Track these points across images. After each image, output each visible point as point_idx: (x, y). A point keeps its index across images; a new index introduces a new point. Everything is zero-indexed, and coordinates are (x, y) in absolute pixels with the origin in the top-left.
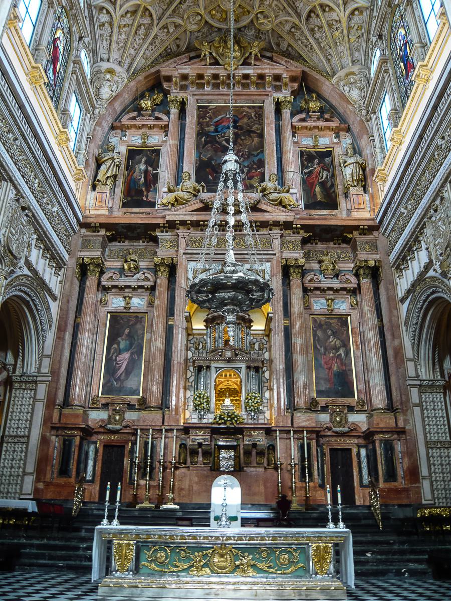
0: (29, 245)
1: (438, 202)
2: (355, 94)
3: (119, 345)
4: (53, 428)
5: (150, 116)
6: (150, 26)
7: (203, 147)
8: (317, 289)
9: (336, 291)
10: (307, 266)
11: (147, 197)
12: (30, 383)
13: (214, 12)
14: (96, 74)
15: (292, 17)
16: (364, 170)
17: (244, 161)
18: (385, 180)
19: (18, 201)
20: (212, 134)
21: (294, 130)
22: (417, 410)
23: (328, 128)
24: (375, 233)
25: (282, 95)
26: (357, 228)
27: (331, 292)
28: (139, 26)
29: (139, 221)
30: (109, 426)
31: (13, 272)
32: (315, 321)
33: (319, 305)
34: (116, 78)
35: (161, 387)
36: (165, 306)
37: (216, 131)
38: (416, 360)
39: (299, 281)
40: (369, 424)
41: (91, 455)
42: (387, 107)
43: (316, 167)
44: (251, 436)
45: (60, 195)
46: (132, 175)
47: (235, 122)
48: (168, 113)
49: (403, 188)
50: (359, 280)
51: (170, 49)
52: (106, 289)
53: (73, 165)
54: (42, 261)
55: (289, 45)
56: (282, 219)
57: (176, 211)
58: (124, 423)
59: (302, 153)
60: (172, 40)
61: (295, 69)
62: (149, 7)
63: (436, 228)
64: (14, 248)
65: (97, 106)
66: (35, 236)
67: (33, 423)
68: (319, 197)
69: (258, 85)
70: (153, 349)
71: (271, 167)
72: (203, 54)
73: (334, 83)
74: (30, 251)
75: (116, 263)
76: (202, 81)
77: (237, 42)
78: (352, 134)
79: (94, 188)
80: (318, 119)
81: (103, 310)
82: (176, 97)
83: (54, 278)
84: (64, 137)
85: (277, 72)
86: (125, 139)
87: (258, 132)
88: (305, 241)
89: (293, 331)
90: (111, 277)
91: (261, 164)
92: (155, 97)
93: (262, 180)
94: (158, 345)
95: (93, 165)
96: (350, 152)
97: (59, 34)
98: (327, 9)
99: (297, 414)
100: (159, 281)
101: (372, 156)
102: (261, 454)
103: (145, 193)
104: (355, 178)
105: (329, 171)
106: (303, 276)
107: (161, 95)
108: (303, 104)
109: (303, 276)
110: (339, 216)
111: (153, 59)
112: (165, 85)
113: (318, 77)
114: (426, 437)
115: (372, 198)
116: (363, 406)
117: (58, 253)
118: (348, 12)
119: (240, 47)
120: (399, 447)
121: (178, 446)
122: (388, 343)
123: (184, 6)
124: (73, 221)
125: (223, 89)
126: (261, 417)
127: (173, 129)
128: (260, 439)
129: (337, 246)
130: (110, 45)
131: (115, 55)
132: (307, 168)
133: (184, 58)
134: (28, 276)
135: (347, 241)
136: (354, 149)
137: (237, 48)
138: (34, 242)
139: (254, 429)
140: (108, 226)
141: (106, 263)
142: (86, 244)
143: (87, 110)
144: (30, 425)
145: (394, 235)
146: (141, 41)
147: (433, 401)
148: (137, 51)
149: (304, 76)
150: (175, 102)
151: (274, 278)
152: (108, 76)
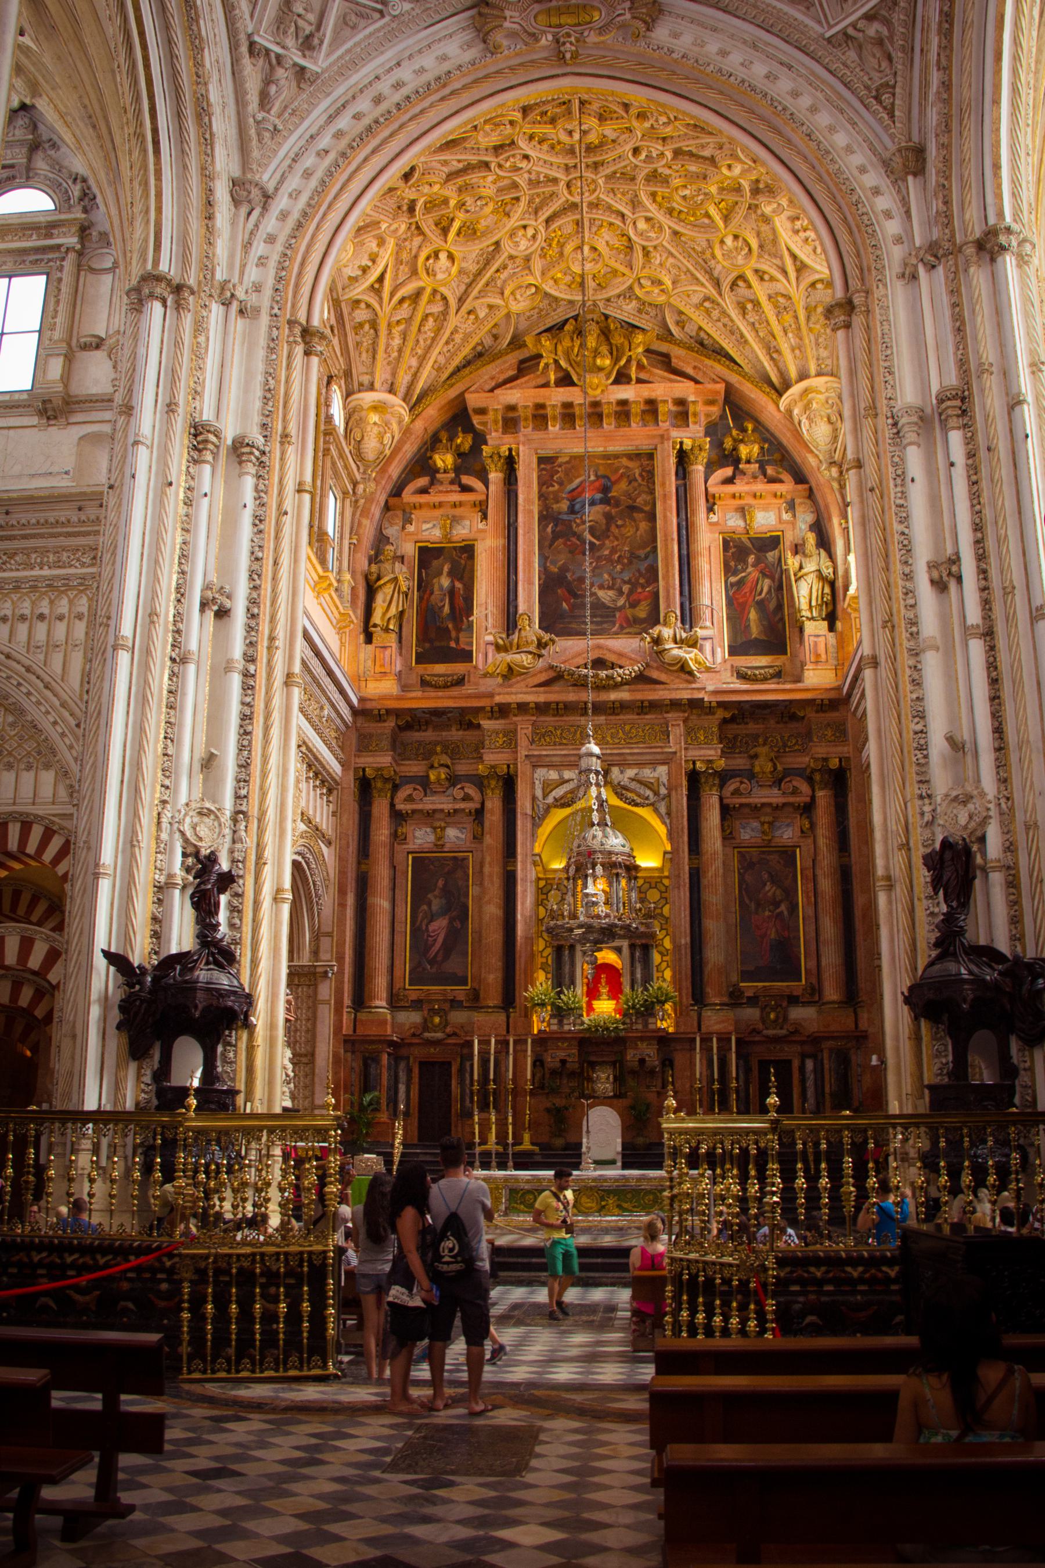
3: (429, 904)
5: (452, 482)
6: (445, 313)
7: (550, 546)
8: (741, 805)
9: (777, 808)
11: (457, 641)
12: (305, 975)
13: (559, 275)
15: (703, 285)
16: (832, 584)
17: (622, 570)
20: (565, 517)
23: (775, 496)
26: (810, 702)
27: (768, 810)
28: (426, 316)
29: (451, 704)
30: (426, 1035)
33: (748, 833)
34: (388, 416)
36: (500, 846)
37: (572, 510)
39: (715, 801)
41: (402, 1076)
43: (751, 572)
44: (636, 1048)
45: (331, 688)
46: (428, 600)
47: (605, 490)
50: (813, 791)
51: (482, 344)
53: (334, 609)
55: (700, 328)
56: (685, 695)
57: (510, 686)
59: (726, 544)
60: (482, 333)
61: (711, 386)
62: (443, 290)
65: (358, 477)
68: (755, 631)
70: (486, 918)
72: (542, 365)
73: (782, 409)
75: (414, 768)
76: (542, 412)
77: (605, 334)
80: (755, 477)
82: (498, 447)
86: (411, 528)
87: (647, 508)
88: (725, 721)
90: (410, 795)
92: (459, 441)
93: (654, 619)
94: (493, 910)
98: (766, 277)
99: (707, 1013)
100: (488, 805)
102: (652, 1072)
103: (453, 634)
104: (814, 603)
105: (773, 580)
106: (722, 786)
107: (469, 439)
109: (722, 786)
111: (450, 369)
112: (476, 420)
116: (812, 994)
117: (329, 774)
118: (803, 286)
119: (610, 344)
123: (504, 275)
126: (651, 1020)
128: (650, 1052)
129: (781, 726)
130: (374, 358)
131: (381, 375)
132: (735, 574)
135: (793, 717)
137: (604, 349)
139: (642, 1039)
140: (397, 713)
141: (397, 769)
143: (345, 493)
146: (429, 342)
148: (422, 359)
150: (496, 458)
151: (673, 793)
152: (374, 418)
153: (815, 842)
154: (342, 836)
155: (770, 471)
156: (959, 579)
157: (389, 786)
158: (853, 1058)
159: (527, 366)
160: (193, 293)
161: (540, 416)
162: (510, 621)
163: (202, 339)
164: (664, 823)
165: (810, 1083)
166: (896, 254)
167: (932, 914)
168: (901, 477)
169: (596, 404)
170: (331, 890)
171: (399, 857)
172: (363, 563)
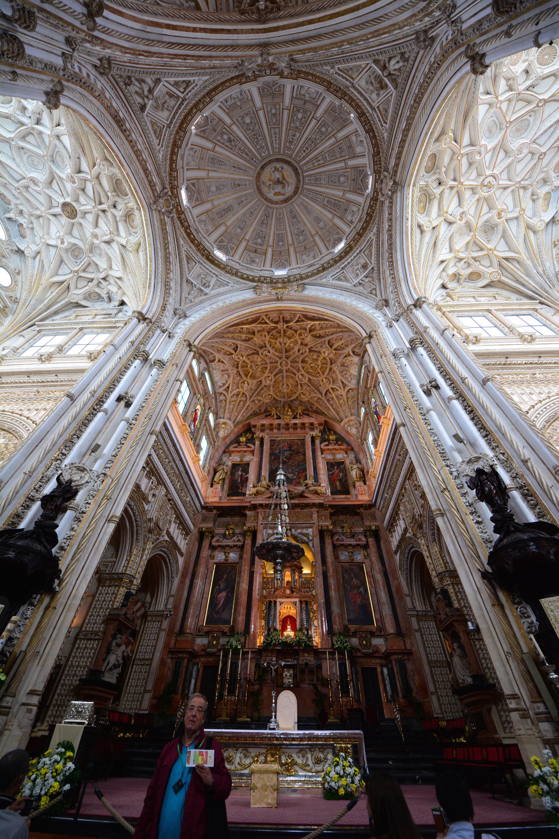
0: (170, 522)
1: (403, 491)
2: (354, 431)
4: (170, 652)
9: (354, 546)
10: (334, 530)
14: (216, 425)
16: (363, 471)
18: (375, 477)
19: (166, 496)
21: (322, 451)
22: (418, 635)
24: (373, 509)
25: (314, 433)
26: (361, 506)
29: (236, 504)
31: (158, 539)
32: (342, 566)
33: (344, 556)
35: (244, 617)
37: (280, 452)
38: (411, 596)
39: (330, 541)
40: (386, 646)
42: (370, 438)
44: (304, 656)
47: (290, 447)
48: (254, 444)
49: (384, 482)
52: (213, 548)
54: (177, 531)
58: (219, 647)
59: (327, 463)
63: (405, 506)
64: (161, 524)
66: (174, 516)
67: (157, 647)
68: (339, 488)
69: (301, 428)
70: (241, 589)
71: (310, 471)
74: (170, 525)
77: (290, 407)
78: (355, 452)
79: (212, 485)
81: (211, 562)
83: (183, 541)
84: (197, 459)
85: (311, 421)
86: (231, 458)
88: (332, 515)
89: (329, 575)
91: (305, 470)
93: (306, 479)
94: (244, 586)
95: (212, 472)
96: (354, 462)
97: (198, 407)
100: (246, 542)
101: (367, 463)
102: (311, 672)
108: (326, 437)
110: (351, 499)
112: (253, 430)
113: (333, 422)
114: (428, 657)
115: (369, 487)
116: (381, 631)
118: (346, 390)
119: (292, 410)
120: (410, 666)
121: (253, 665)
122: (391, 583)
124: (198, 505)
125: (282, 431)
127: (257, 452)
128: (309, 658)
133: (263, 416)
134: (167, 541)
136: (356, 460)
138: (173, 520)
142: (204, 520)
143: (211, 444)
144: (155, 649)
145: (384, 510)
147: (428, 627)
148: (239, 413)
149: (326, 423)
153: (371, 561)
154: (189, 553)
155: (339, 443)
156: (437, 387)
157: (210, 535)
158: (407, 665)
159: (267, 414)
160: (151, 322)
161: (271, 426)
162: (259, 480)
163: (151, 333)
164: (311, 551)
165: (387, 682)
166: (384, 324)
167: (478, 522)
168: (400, 367)
169: (287, 424)
170: (179, 575)
171: (210, 565)
172: (214, 464)
